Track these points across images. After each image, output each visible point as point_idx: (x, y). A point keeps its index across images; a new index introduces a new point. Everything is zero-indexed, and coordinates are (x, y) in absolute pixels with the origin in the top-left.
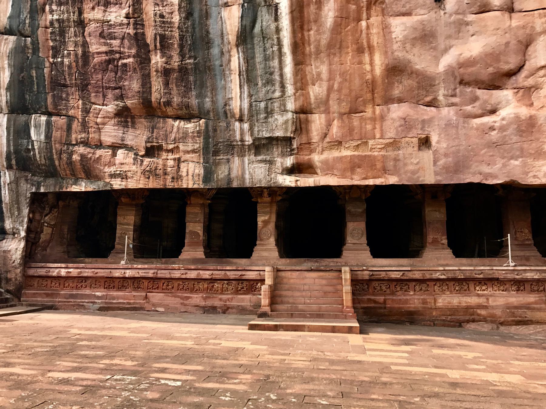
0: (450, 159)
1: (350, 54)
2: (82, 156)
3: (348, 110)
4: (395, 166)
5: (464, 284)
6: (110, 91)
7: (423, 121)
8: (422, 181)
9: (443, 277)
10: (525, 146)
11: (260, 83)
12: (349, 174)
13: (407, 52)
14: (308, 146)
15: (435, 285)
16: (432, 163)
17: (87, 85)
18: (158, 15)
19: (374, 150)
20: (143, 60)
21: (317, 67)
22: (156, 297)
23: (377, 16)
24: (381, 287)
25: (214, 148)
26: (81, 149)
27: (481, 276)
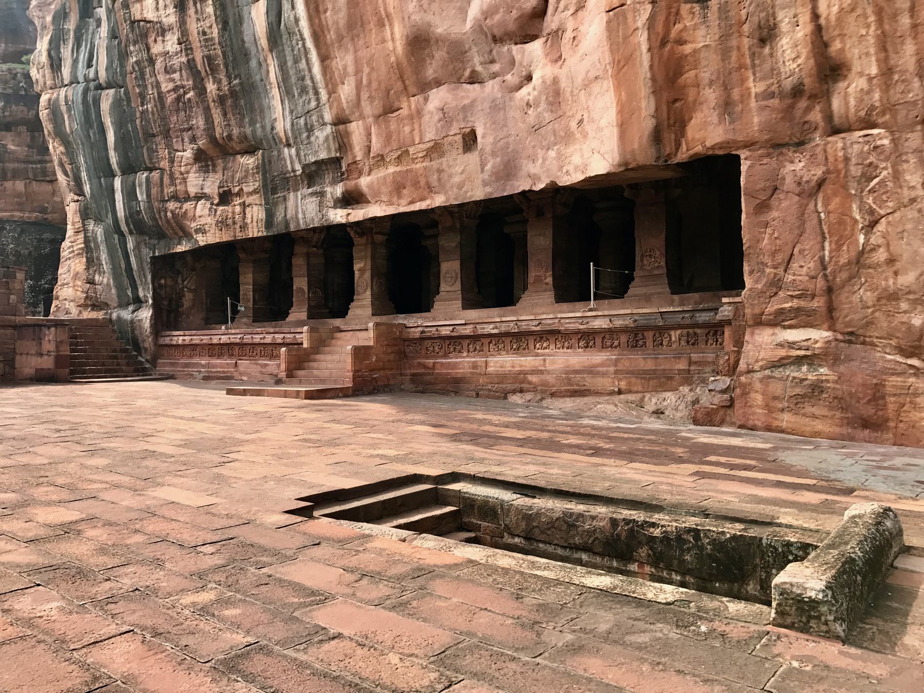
0: (498, 159)
1: (374, 31)
2: (172, 212)
3: (381, 110)
4: (439, 180)
6: (185, 133)
7: (464, 109)
8: (471, 197)
10: (557, 126)
11: (296, 94)
12: (395, 199)
13: (425, 11)
15: (490, 343)
21: (342, 59)
22: (244, 364)
25: (274, 185)
26: (171, 205)
27: (538, 328)
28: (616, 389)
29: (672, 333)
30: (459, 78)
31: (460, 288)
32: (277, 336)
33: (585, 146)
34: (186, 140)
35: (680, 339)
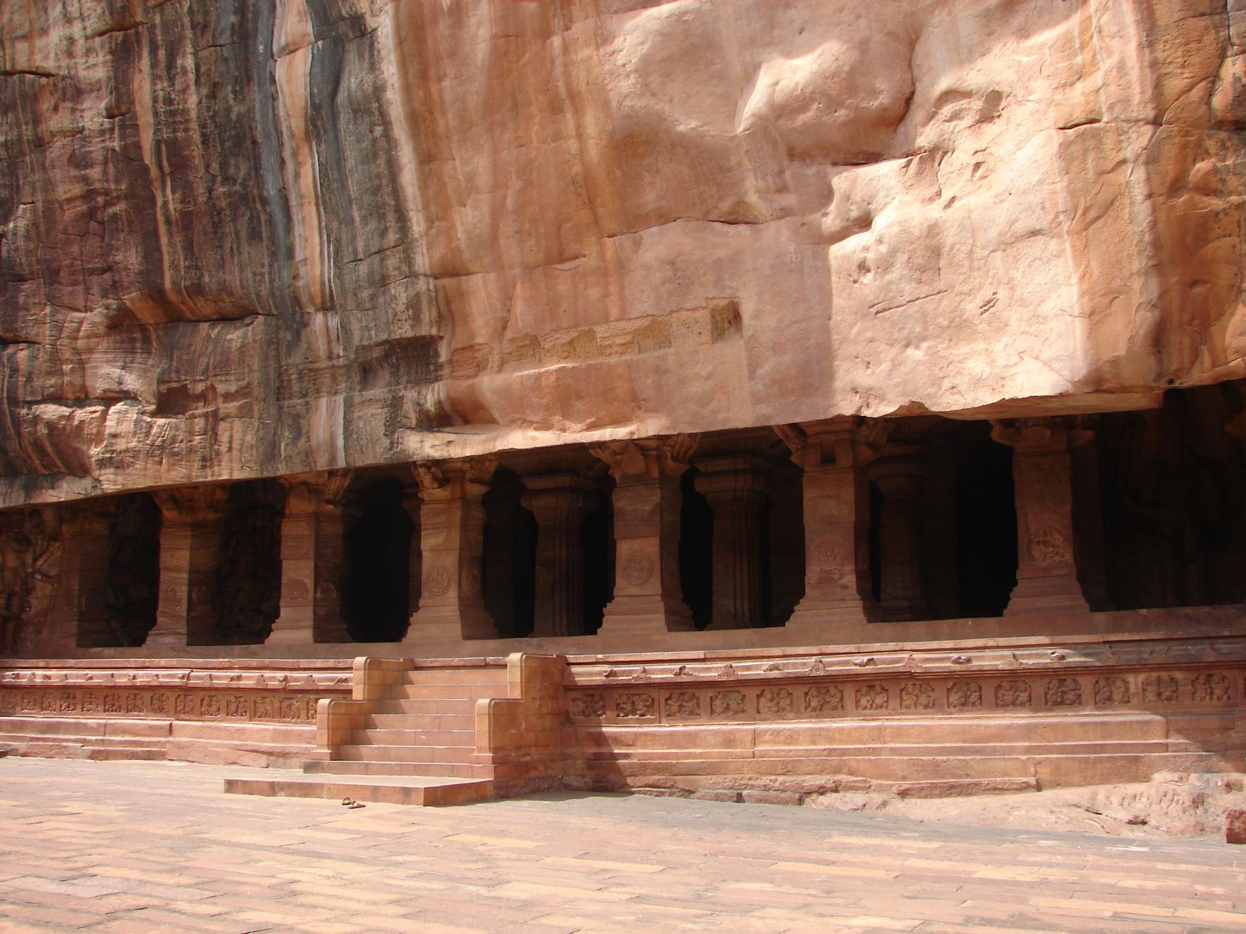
0: (787, 358)
1: (537, 119)
4: (658, 387)
5: (833, 691)
6: (94, 278)
7: (718, 263)
9: (775, 674)
10: (930, 307)
11: (357, 219)
13: (653, 95)
14: (469, 353)
16: (746, 373)
17: (57, 272)
18: (161, 100)
19: (609, 351)
20: (143, 202)
22: (188, 729)
23: (586, 18)
24: (633, 703)
26: (51, 411)
28: (1032, 781)
29: (1131, 678)
30: (708, 212)
31: (659, 590)
32: (267, 674)
33: (1000, 346)
34: (96, 290)
35: (1144, 690)
